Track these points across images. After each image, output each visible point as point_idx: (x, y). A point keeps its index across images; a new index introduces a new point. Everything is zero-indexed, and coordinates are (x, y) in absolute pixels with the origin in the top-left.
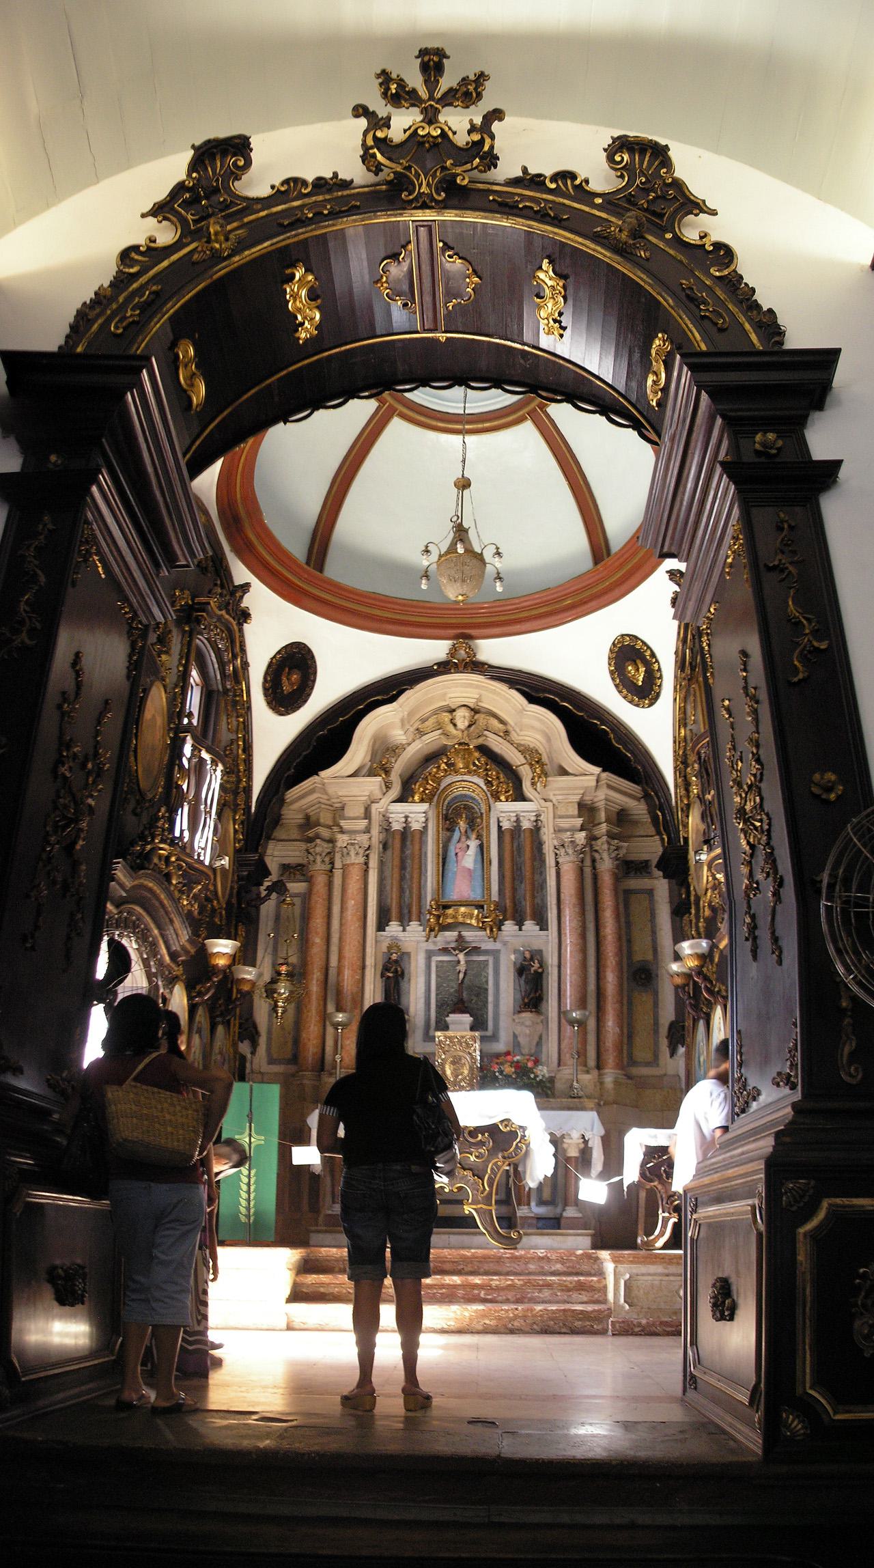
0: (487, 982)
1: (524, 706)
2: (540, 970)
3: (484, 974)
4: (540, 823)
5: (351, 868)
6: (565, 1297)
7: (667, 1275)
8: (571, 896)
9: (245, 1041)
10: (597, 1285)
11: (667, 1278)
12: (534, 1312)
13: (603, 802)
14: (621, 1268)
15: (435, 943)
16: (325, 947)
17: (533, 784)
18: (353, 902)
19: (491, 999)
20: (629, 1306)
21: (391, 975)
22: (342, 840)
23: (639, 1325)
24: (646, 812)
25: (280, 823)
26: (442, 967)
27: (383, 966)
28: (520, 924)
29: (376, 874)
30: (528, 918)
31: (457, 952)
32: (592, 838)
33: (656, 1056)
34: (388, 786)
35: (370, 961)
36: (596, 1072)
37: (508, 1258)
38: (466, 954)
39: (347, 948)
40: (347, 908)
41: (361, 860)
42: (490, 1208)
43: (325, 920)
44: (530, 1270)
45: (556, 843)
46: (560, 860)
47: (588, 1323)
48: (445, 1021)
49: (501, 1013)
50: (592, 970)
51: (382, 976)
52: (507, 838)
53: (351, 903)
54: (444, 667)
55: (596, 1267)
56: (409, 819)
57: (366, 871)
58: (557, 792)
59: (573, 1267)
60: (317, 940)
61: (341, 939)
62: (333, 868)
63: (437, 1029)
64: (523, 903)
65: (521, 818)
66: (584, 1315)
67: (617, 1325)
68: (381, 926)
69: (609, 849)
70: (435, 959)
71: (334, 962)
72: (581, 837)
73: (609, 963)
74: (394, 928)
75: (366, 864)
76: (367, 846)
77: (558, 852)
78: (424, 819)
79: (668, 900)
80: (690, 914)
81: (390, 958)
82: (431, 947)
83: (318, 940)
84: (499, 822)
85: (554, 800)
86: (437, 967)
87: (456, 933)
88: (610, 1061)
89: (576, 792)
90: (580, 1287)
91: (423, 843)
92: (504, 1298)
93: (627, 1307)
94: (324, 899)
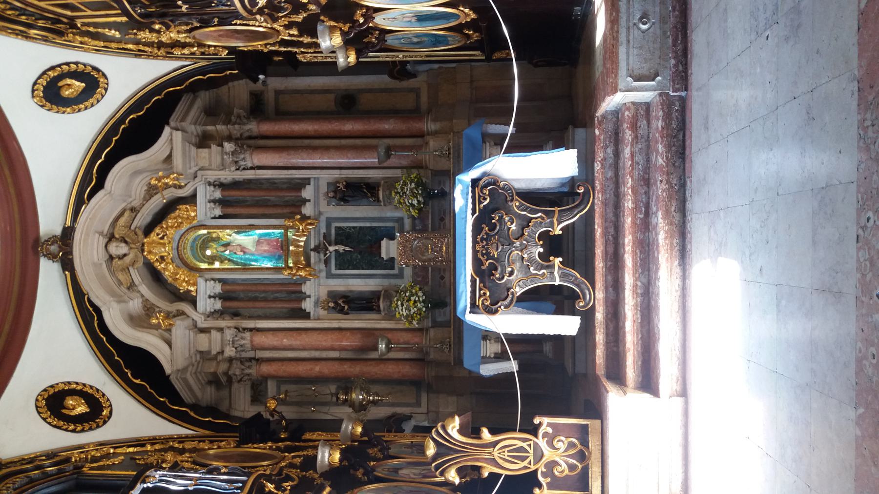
0: (354, 228)
1: (106, 193)
2: (344, 183)
3: (348, 230)
4: (216, 183)
5: (255, 343)
6: (643, 140)
7: (628, 41)
8: (280, 157)
9: (404, 428)
10: (632, 111)
11: (631, 41)
12: (664, 164)
13: (198, 127)
14: (621, 85)
15: (320, 271)
16: (323, 362)
17: (180, 187)
18: (284, 340)
19: (368, 224)
20: (658, 75)
21: (346, 307)
22: (230, 352)
23: (676, 66)
24: (207, 93)
25: (215, 406)
26: (338, 266)
27: (339, 313)
28: (305, 201)
29: (261, 321)
30: (299, 194)
31: (328, 252)
32: (229, 138)
33: (411, 90)
34: (181, 313)
35: (335, 324)
36: (428, 138)
37: (602, 195)
38: (330, 245)
39: (324, 344)
40: (290, 345)
41: (247, 335)
42: (557, 212)
43: (300, 363)
44: (613, 175)
45: (233, 168)
46: (250, 165)
47: (673, 115)
48: (386, 261)
49: (379, 216)
50: (344, 142)
51: (347, 314)
52: (230, 211)
53: (286, 342)
54: (67, 265)
55: (610, 117)
56: (212, 294)
57: (258, 330)
58: (188, 166)
59: (610, 138)
60: (318, 369)
61: (317, 349)
62: (254, 359)
63: (393, 268)
64: (287, 199)
65: (212, 198)
66: (667, 117)
67: (677, 86)
68: (306, 316)
69: (239, 124)
70: (334, 271)
71: (335, 354)
72: (229, 146)
73: (337, 128)
74: (308, 305)
75: (251, 330)
76: (235, 330)
77: (242, 167)
78: (212, 282)
79: (284, 78)
80: (296, 52)
81: (333, 308)
82: (323, 274)
83: (317, 369)
84: (215, 218)
85: (196, 169)
86: (340, 269)
87: (312, 254)
88: (417, 126)
89: (187, 148)
90: (634, 127)
91: (234, 282)
92: (644, 196)
93: (659, 78)
94: (282, 366)
